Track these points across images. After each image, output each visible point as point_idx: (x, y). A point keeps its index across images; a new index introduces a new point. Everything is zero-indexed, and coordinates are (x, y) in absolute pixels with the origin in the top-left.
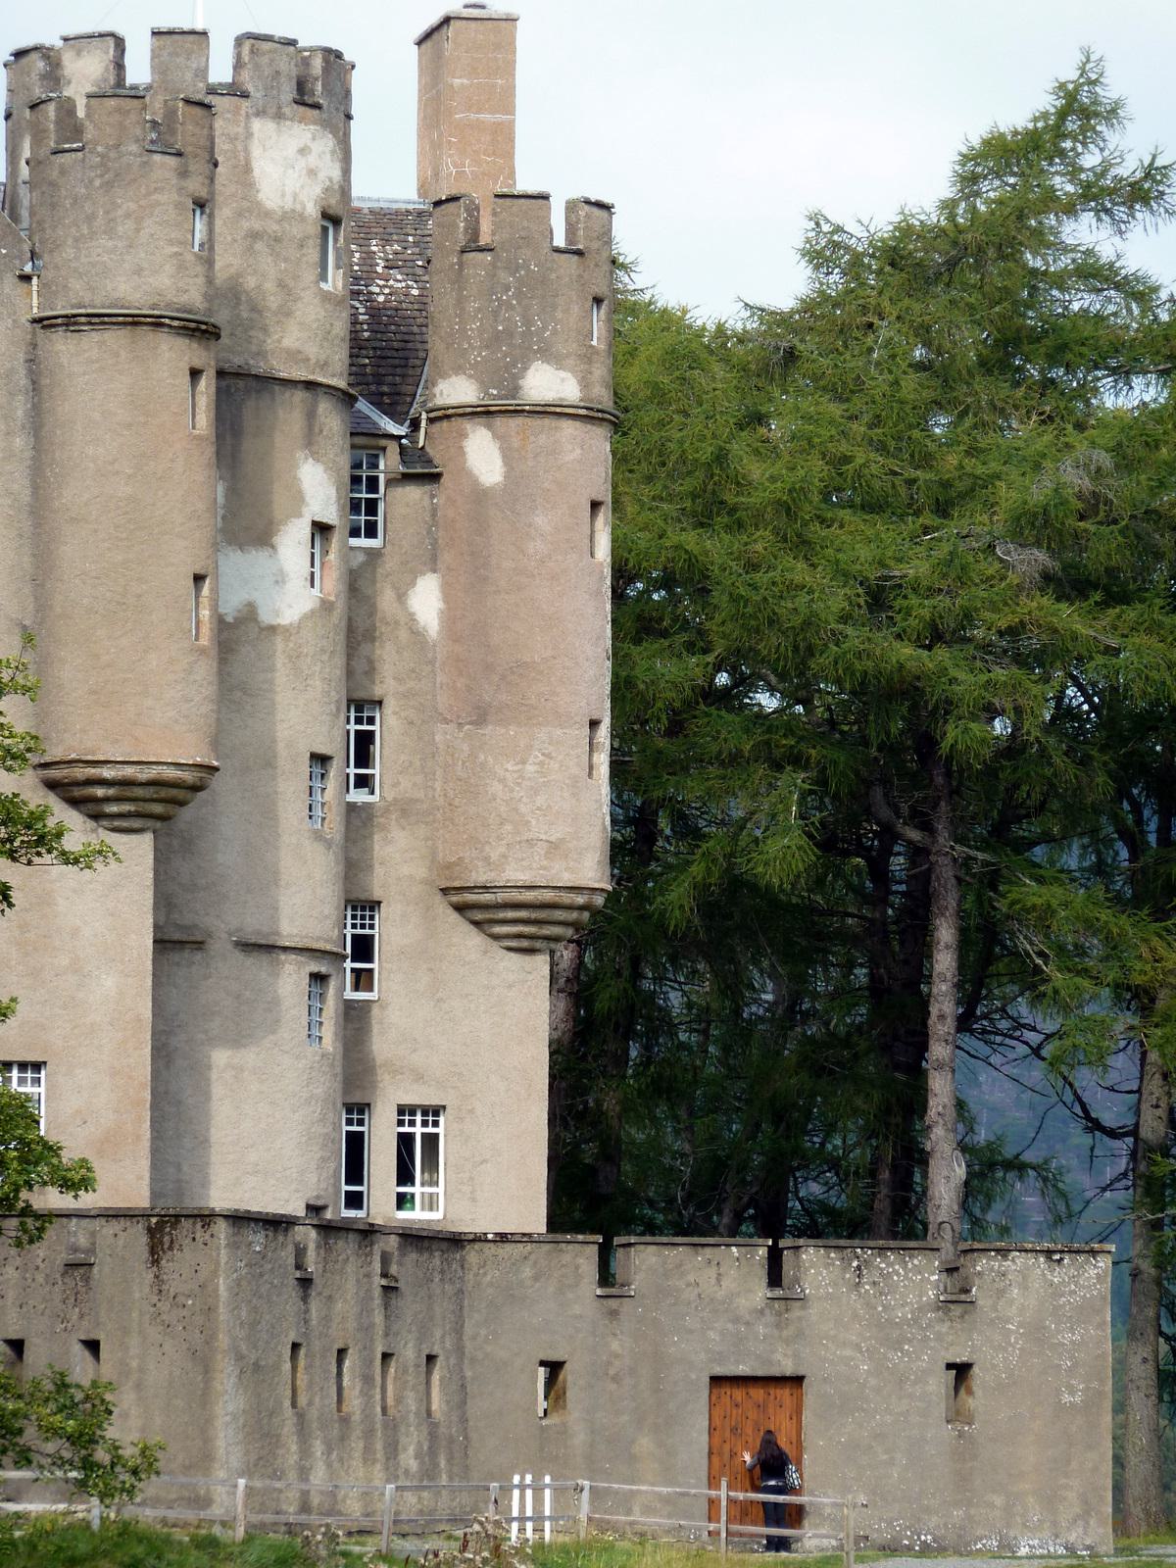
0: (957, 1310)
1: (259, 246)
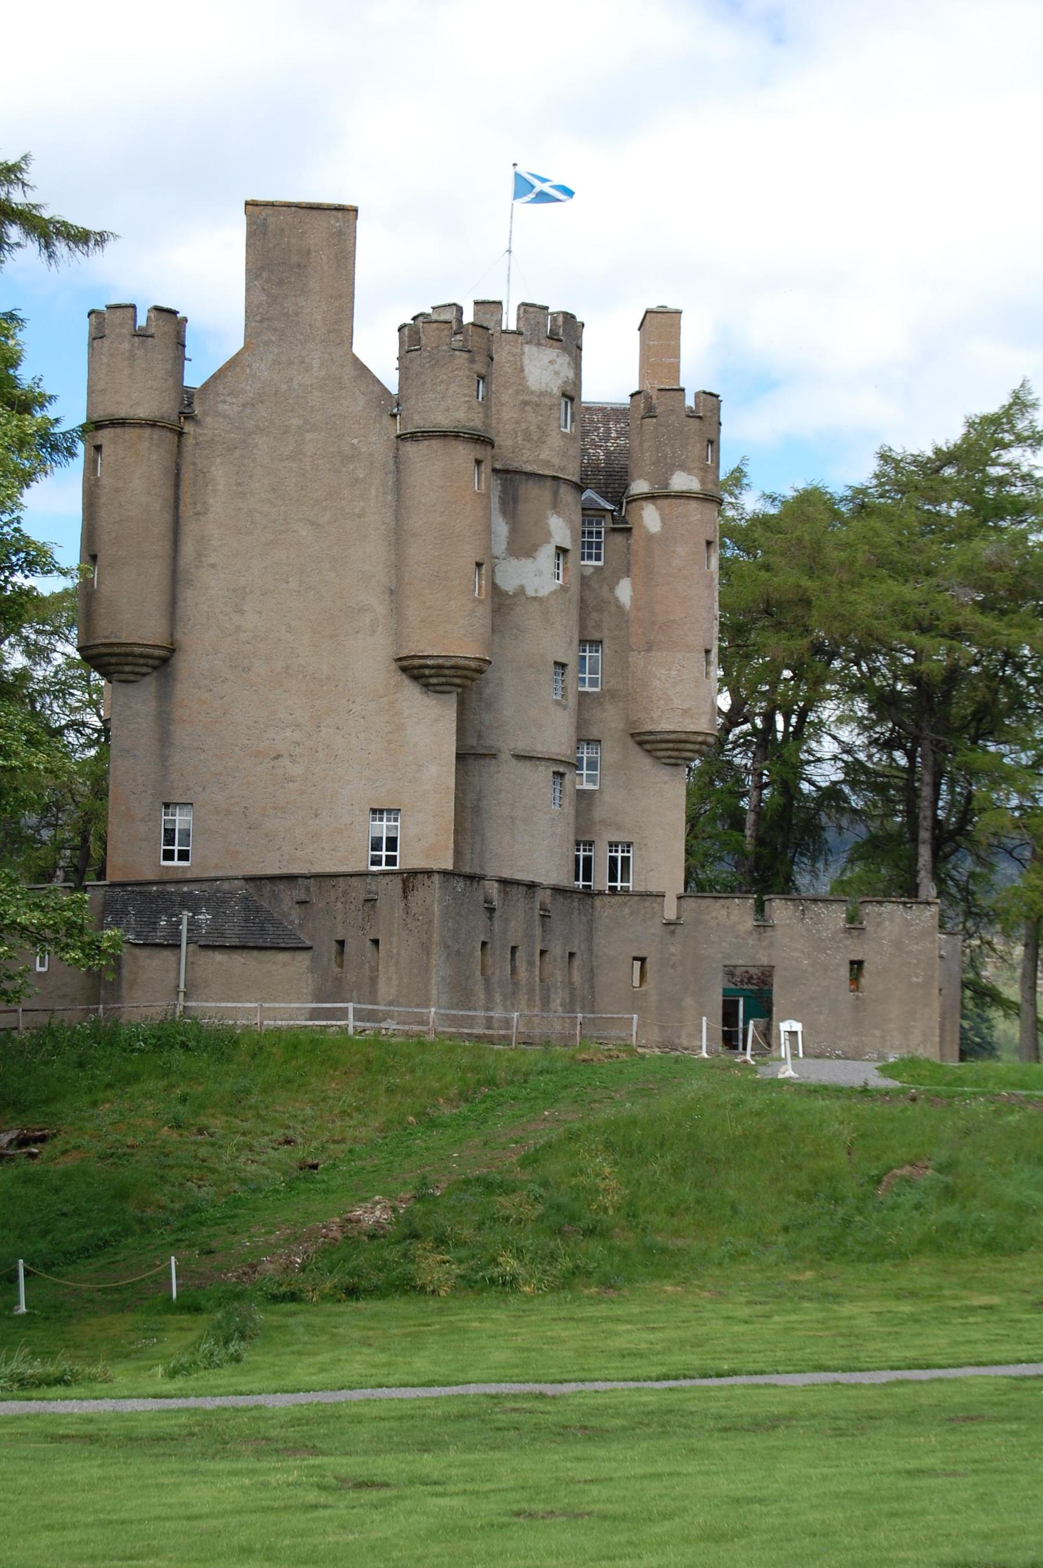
0: (855, 933)
1: (527, 408)
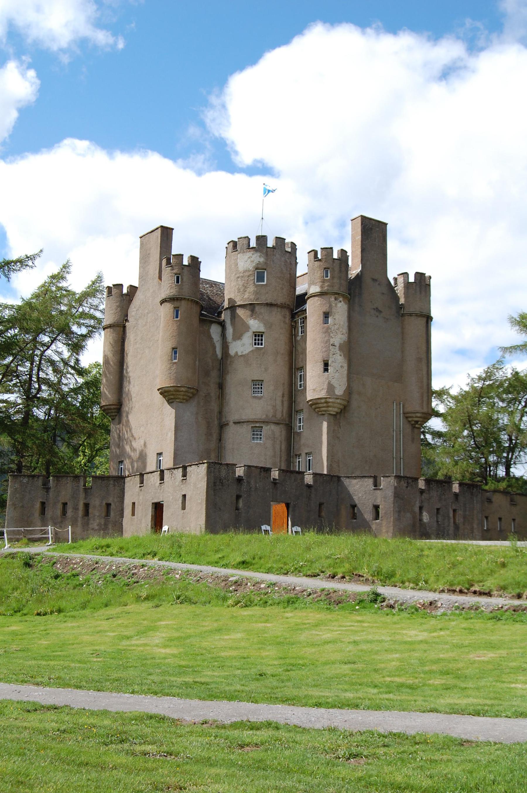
1: (239, 279)
